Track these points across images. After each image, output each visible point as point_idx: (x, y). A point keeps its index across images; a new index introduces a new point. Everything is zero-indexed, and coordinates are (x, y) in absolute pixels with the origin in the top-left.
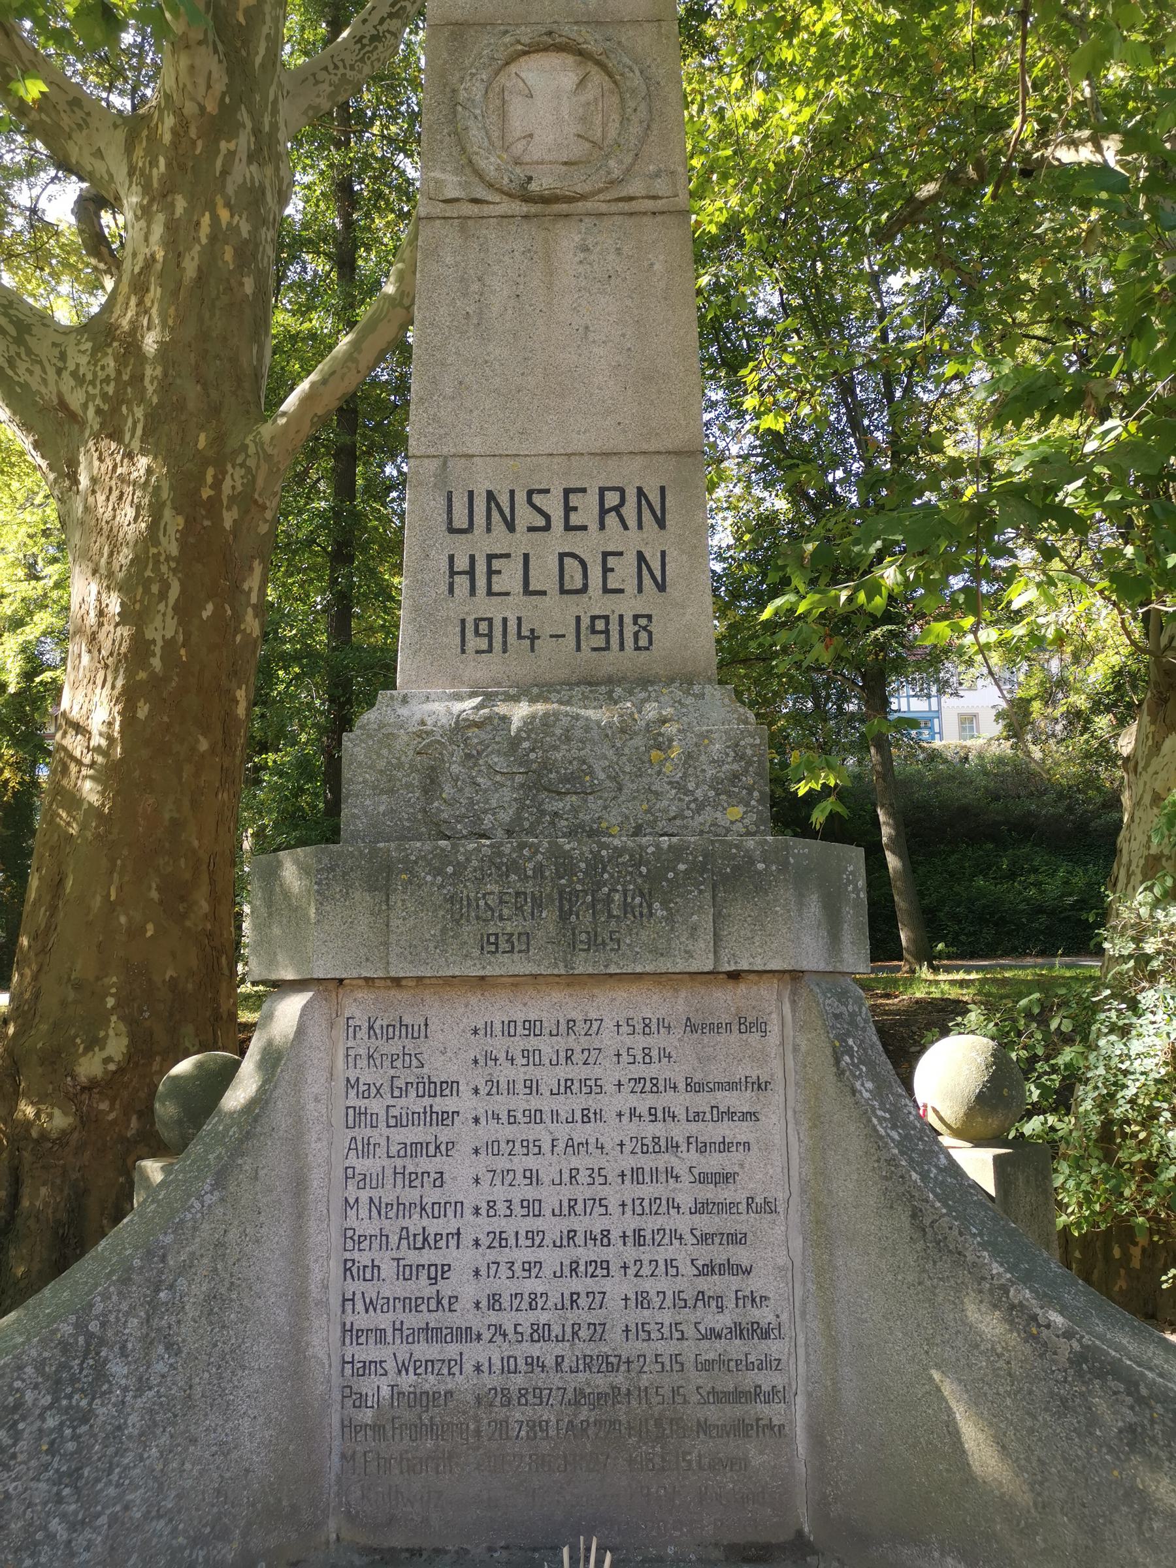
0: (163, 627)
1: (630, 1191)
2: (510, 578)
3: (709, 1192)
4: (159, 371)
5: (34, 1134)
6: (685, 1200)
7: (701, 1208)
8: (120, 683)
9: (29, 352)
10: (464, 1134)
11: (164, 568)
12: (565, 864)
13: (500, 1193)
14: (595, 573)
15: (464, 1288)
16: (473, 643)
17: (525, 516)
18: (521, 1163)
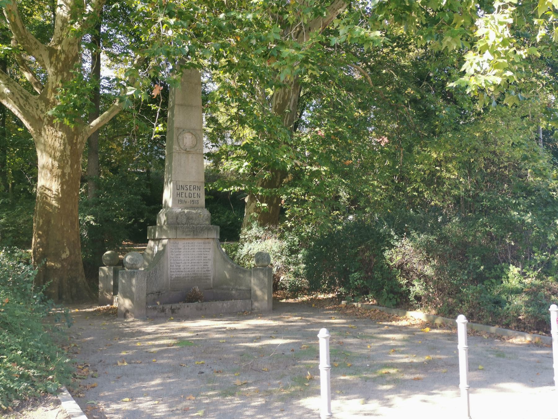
0: (68, 170)
2: (183, 195)
5: (54, 268)
8: (60, 181)
9: (29, 103)
10: (182, 253)
12: (193, 227)
15: (182, 267)
17: (185, 188)
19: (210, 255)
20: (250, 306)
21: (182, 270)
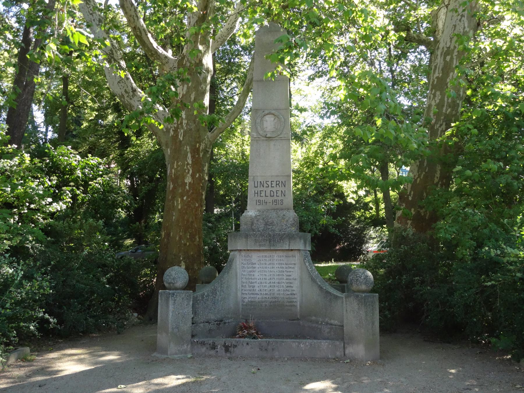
1: (278, 277)
2: (263, 194)
3: (288, 277)
4: (186, 121)
6: (285, 278)
7: (287, 279)
10: (257, 270)
11: (188, 166)
12: (270, 235)
14: (275, 194)
15: (257, 289)
16: (258, 203)
17: (265, 185)
18: (264, 273)
19: (296, 273)
21: (257, 292)
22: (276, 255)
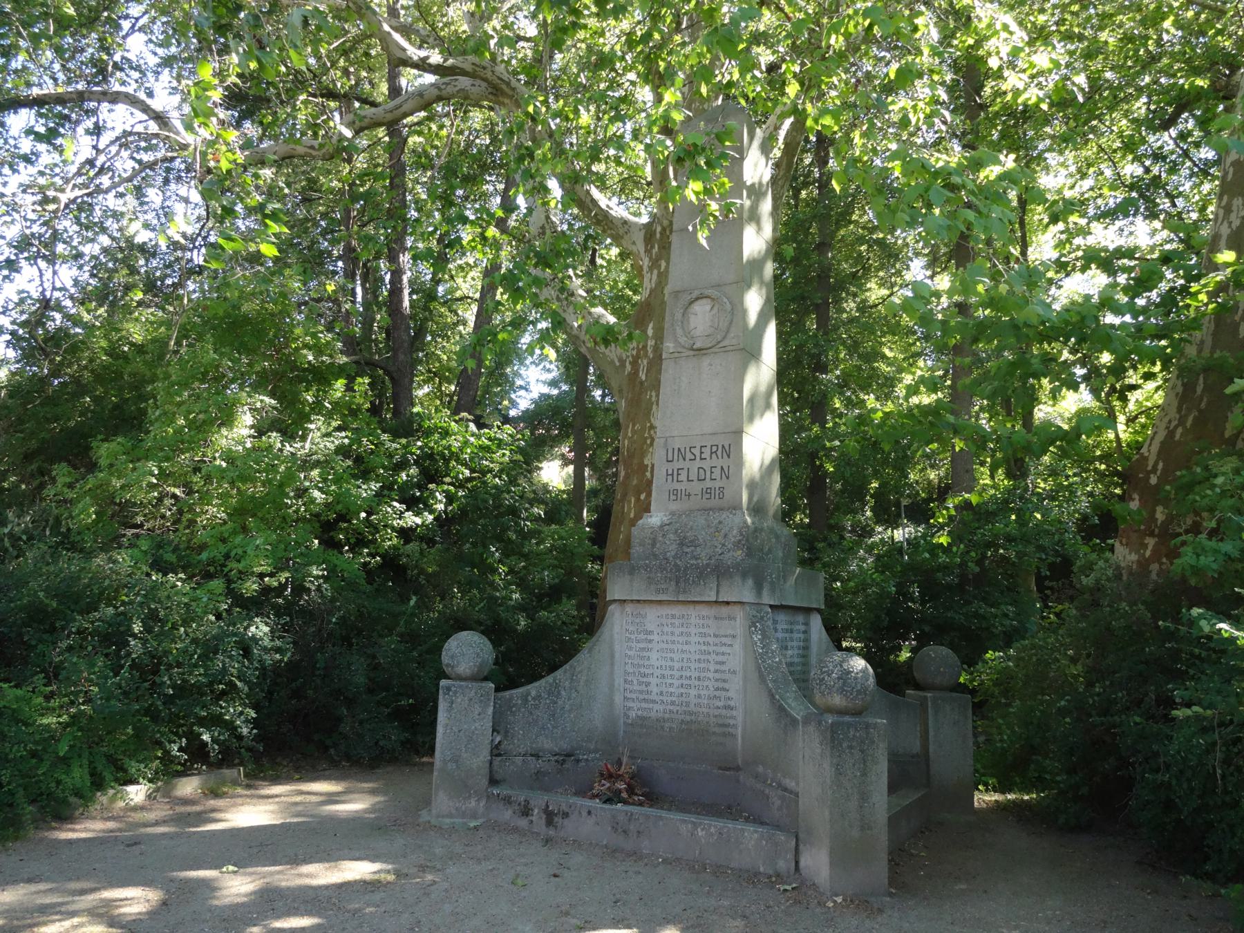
1: (697, 665)
2: (683, 477)
3: (718, 667)
6: (712, 669)
7: (716, 671)
10: (654, 645)
13: (664, 663)
14: (708, 473)
17: (689, 456)
19: (736, 656)
20: (790, 856)
22: (694, 614)
